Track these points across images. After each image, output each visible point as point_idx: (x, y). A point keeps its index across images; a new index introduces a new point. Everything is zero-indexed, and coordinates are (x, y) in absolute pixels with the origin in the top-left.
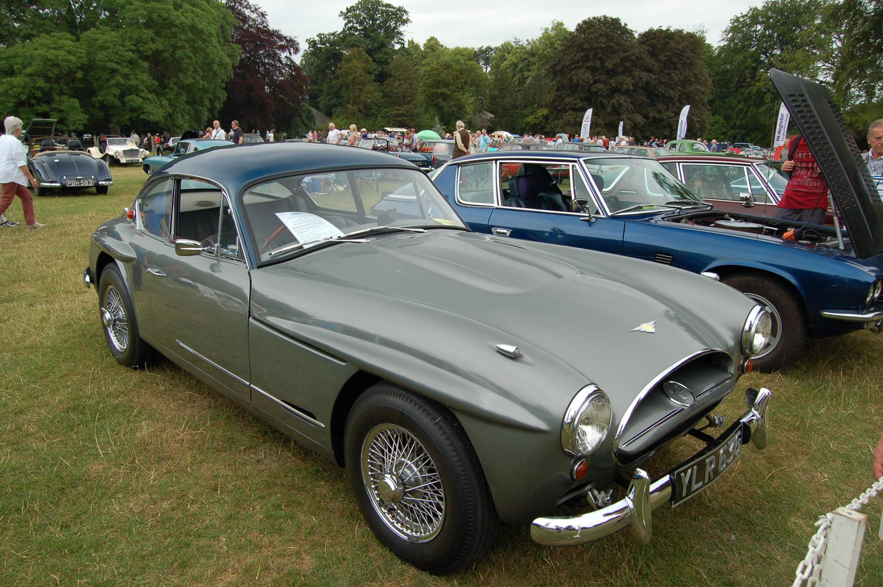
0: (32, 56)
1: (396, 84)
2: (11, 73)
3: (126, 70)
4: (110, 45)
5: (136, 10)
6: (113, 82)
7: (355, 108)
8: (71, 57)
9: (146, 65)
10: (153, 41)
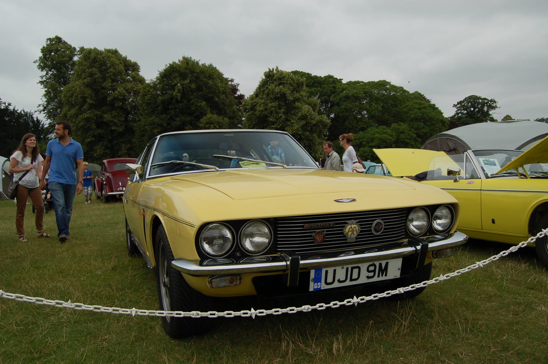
4: (406, 131)
5: (416, 113)
9: (420, 140)
10: (424, 128)
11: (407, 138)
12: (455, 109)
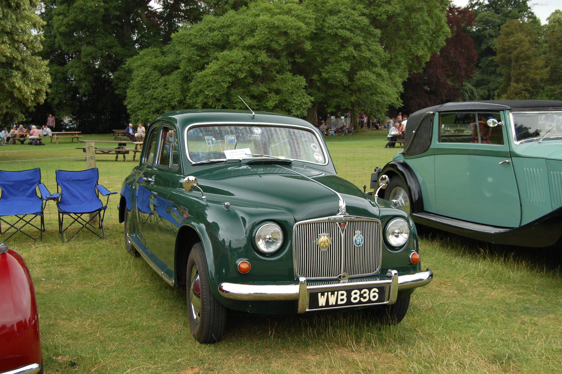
0: (253, 23)
2: (224, 45)
3: (360, 40)
4: (342, 8)
6: (344, 54)
7: (521, 85)
8: (301, 24)
9: (378, 32)
11: (343, 28)
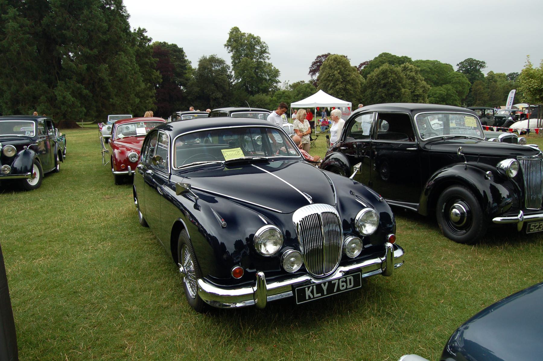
1: (494, 93)
12: (458, 67)
